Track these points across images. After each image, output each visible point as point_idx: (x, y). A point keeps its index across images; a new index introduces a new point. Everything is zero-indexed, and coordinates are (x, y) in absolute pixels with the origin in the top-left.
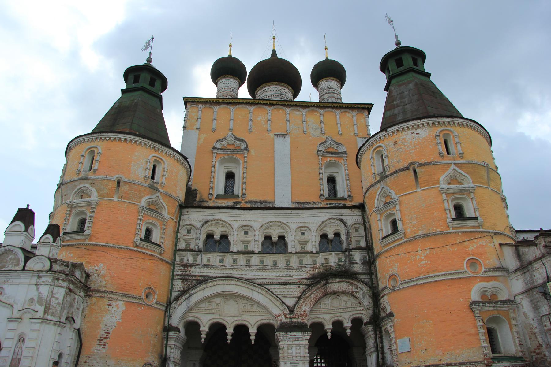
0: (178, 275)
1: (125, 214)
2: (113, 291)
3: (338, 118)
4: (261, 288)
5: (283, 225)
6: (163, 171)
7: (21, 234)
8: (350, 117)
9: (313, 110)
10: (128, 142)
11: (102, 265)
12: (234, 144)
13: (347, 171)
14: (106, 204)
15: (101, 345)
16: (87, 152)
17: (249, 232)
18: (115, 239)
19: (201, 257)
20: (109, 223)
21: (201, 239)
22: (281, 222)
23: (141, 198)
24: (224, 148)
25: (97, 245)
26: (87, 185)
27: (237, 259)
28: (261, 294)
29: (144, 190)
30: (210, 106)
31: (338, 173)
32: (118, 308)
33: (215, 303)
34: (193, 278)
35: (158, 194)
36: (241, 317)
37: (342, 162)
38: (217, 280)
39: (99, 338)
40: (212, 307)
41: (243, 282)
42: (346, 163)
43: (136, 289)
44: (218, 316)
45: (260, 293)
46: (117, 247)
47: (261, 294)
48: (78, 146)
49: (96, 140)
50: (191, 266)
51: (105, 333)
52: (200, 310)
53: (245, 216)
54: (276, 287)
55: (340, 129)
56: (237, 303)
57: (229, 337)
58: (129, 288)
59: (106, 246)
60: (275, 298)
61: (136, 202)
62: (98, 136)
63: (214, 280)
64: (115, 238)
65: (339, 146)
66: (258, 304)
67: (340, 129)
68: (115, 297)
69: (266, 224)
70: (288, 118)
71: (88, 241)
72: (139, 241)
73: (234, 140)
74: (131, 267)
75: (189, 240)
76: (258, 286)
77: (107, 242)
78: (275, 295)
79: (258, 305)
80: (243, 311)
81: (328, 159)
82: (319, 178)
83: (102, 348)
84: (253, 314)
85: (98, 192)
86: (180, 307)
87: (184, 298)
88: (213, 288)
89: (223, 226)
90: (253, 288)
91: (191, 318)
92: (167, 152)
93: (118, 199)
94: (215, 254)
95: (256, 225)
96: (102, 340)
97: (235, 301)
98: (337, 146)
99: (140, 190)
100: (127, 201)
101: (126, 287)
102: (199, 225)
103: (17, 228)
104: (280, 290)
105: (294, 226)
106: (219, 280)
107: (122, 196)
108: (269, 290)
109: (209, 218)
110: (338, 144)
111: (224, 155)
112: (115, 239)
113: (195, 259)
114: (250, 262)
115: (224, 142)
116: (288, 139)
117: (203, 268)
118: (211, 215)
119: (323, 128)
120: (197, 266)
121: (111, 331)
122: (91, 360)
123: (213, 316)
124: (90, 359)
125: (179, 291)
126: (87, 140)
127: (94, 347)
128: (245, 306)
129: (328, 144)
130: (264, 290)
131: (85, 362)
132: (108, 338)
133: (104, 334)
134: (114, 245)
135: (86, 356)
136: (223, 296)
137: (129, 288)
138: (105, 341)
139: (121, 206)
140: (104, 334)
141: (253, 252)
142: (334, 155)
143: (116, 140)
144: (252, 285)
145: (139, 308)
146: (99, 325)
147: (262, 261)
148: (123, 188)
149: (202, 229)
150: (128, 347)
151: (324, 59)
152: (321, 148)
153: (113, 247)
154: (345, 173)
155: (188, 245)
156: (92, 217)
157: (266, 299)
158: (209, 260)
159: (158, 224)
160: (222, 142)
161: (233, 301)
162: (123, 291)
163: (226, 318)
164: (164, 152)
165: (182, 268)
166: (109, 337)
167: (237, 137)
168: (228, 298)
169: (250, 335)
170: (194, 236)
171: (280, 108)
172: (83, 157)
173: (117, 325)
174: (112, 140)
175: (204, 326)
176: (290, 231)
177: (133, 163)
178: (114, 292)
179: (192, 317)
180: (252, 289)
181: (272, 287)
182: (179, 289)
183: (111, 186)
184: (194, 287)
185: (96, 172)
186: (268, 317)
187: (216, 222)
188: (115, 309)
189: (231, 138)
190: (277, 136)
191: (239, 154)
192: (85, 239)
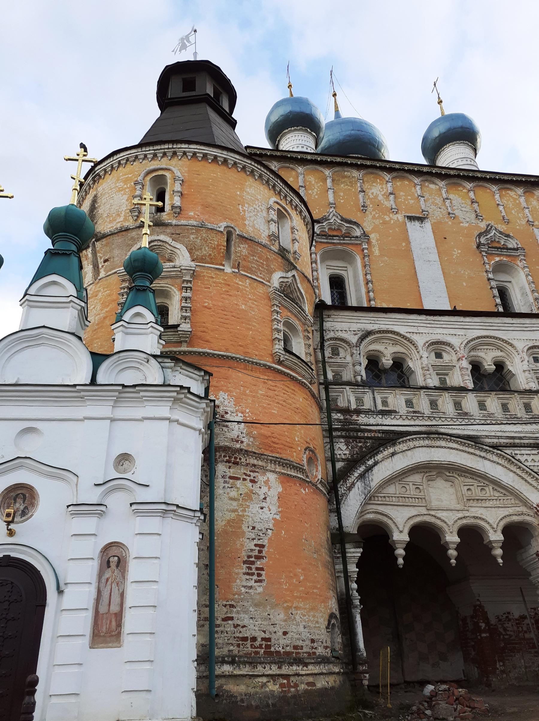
0: (337, 430)
1: (250, 299)
2: (254, 450)
3: (497, 196)
4: (497, 454)
5: (501, 343)
6: (292, 233)
7: (71, 301)
8: (515, 196)
9: (455, 184)
10: (230, 166)
11: (226, 397)
12: (340, 230)
13: (530, 277)
14: (212, 278)
15: (253, 574)
16: (148, 178)
17: (444, 354)
18: (240, 346)
19: (371, 396)
20: (225, 313)
21: (362, 364)
22: (496, 338)
23: (271, 272)
24: (323, 233)
25: (209, 354)
26: (162, 237)
27: (437, 400)
28: (500, 464)
29: (274, 259)
30: (291, 166)
31: (510, 282)
32: (269, 488)
33: (413, 484)
34: (366, 435)
35: (294, 272)
36: (468, 510)
37: (519, 264)
38: (412, 439)
39: (246, 558)
40: (408, 492)
41: (461, 442)
42: (526, 265)
43: (292, 448)
44: (424, 511)
45: (498, 463)
46: (248, 361)
47: (500, 464)
48: (120, 169)
49: (162, 157)
50: (358, 412)
51: (256, 545)
52: (387, 499)
53: (433, 326)
54: (523, 452)
55: (504, 214)
56: (451, 483)
57: (452, 553)
58: (282, 446)
59: (228, 357)
60: (527, 472)
61: (263, 279)
62: (168, 148)
63: (408, 438)
64: (240, 343)
65: (509, 239)
66: (496, 483)
67: (504, 214)
68: (260, 463)
69: (472, 340)
70: (419, 192)
71: (187, 347)
72: (283, 352)
73: (340, 222)
74: (278, 403)
75: (340, 366)
76: (491, 449)
77: (227, 350)
78: (526, 466)
79: (496, 487)
80: (469, 500)
81: (497, 259)
82: (489, 287)
83: (256, 581)
84: (488, 504)
85: (190, 251)
86: (352, 493)
87: (356, 475)
88: (409, 453)
89: (396, 343)
90: (483, 454)
91: (371, 516)
92: (292, 200)
93: (233, 270)
94: (398, 391)
95: (455, 341)
96: (253, 563)
97: (446, 480)
98: (506, 238)
99: (267, 258)
100: (249, 275)
101: (277, 444)
102: (354, 339)
103: (52, 291)
104: (532, 457)
105: (521, 346)
106: (416, 438)
107: (238, 265)
108: (513, 457)
109: (370, 327)
110: (508, 236)
111: (329, 245)
112: (240, 346)
113: (359, 400)
114: (461, 407)
115: (324, 224)
116: (428, 225)
117: (380, 416)
118: (373, 322)
119: (478, 211)
120: (368, 412)
121: (265, 542)
122: (238, 612)
123: (413, 512)
124: (235, 610)
125: (343, 460)
126: (142, 157)
127: (238, 581)
128: (468, 489)
129: (492, 234)
130: (504, 457)
131: (225, 619)
132: (262, 557)
133: (254, 548)
134: (242, 357)
135: (225, 603)
136: (425, 470)
137: (282, 446)
138: (258, 564)
139: (241, 283)
140: (254, 548)
141: (463, 389)
142: (505, 252)
143: (207, 159)
144: (479, 448)
145: (302, 490)
146: (240, 527)
147: (482, 406)
148: (239, 249)
149: (361, 347)
150: (301, 578)
151: (440, 116)
152: (483, 240)
153: (240, 359)
154: (528, 281)
155: (337, 374)
156: (189, 297)
157: (511, 474)
158: (387, 402)
159: (300, 328)
160: (320, 225)
161: (444, 482)
162: (272, 451)
163: (440, 514)
164: (289, 199)
165: (339, 416)
166: (264, 554)
167: (344, 217)
168: (435, 473)
169: (492, 548)
170: (349, 359)
171: (403, 178)
172: (141, 186)
173: (274, 525)
174: (200, 159)
175: (401, 532)
176: (516, 354)
177: (246, 205)
178: (258, 454)
179: (373, 512)
180: (480, 456)
181: (517, 452)
182: (343, 457)
183: (216, 243)
184: (374, 451)
185: (179, 214)
186: (518, 509)
187: (383, 335)
188: (265, 489)
189: (334, 218)
190: (410, 219)
191: (352, 244)
192: (181, 342)
